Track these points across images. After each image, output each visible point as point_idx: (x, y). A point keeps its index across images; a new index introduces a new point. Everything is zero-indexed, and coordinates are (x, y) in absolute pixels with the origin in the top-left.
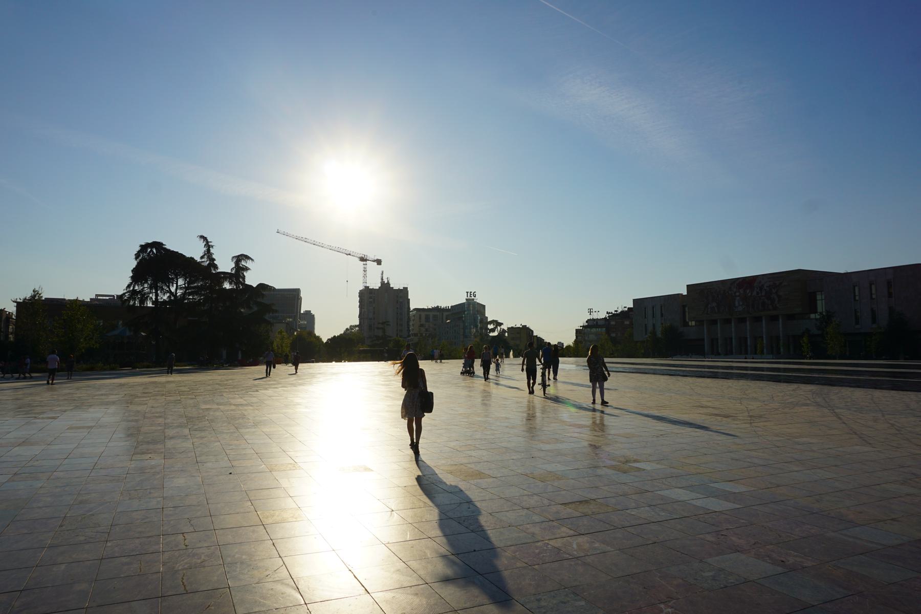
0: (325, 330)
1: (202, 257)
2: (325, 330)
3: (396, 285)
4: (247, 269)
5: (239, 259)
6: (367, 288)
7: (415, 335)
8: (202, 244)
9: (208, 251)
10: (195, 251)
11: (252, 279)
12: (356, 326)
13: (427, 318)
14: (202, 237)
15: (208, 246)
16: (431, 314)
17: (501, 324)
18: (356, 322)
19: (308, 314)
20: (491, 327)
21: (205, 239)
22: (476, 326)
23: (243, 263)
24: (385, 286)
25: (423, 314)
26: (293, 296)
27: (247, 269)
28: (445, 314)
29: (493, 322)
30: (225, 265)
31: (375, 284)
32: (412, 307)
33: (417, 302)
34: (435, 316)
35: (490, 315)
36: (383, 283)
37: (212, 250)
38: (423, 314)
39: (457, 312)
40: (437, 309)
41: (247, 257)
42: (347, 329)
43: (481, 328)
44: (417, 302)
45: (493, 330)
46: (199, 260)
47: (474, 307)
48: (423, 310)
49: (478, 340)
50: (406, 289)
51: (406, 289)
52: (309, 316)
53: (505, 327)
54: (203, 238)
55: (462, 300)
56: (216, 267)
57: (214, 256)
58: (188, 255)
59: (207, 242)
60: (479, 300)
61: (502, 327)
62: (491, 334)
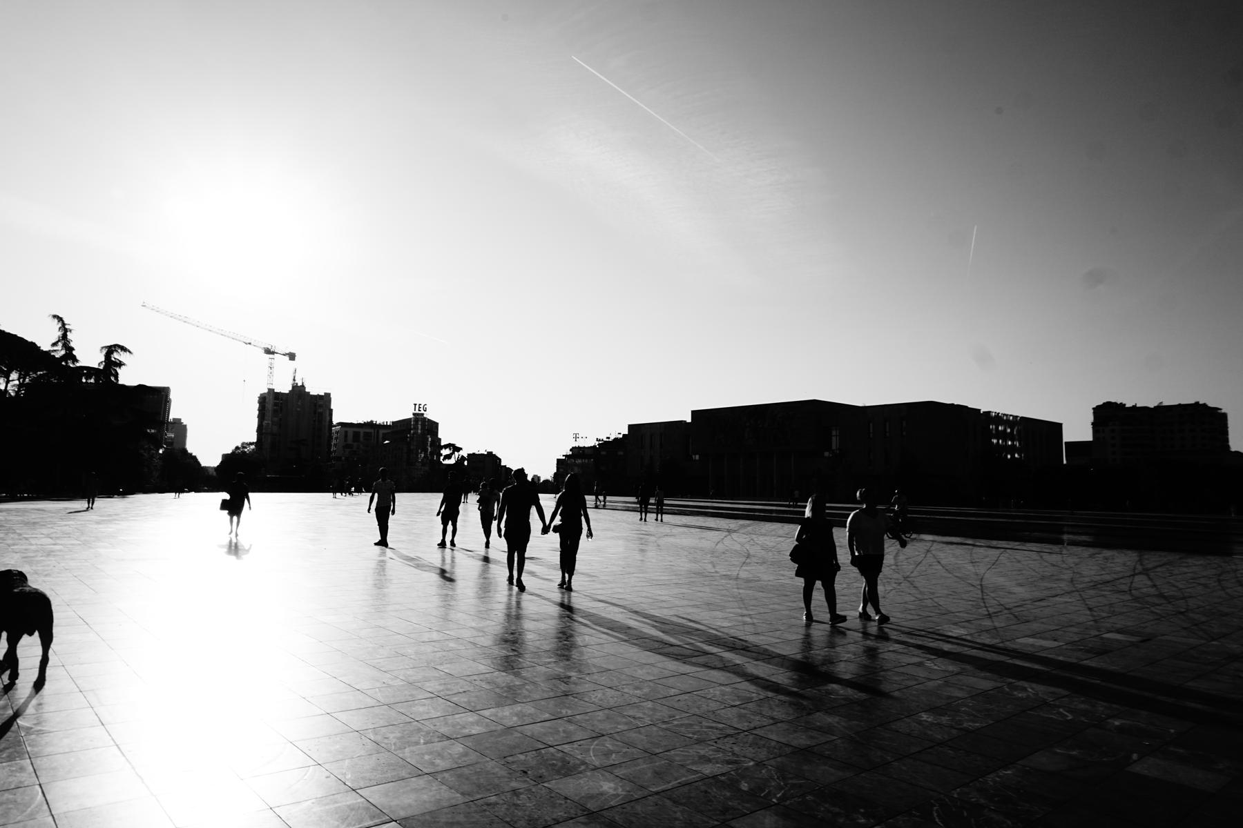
0: (208, 447)
1: (54, 344)
2: (208, 447)
3: (314, 389)
4: (120, 364)
5: (111, 350)
6: (271, 391)
7: (338, 459)
8: (56, 325)
9: (64, 336)
10: (44, 338)
11: (128, 377)
12: (251, 444)
13: (356, 435)
14: (55, 316)
15: (65, 330)
16: (362, 431)
17: (459, 449)
18: (253, 438)
19: (177, 422)
20: (445, 452)
21: (60, 319)
22: (425, 450)
23: (115, 356)
24: (298, 390)
25: (350, 431)
26: (156, 398)
27: (120, 364)
28: (381, 432)
29: (446, 446)
30: (89, 356)
31: (285, 388)
32: (335, 420)
33: (341, 414)
34: (366, 434)
35: (445, 436)
36: (295, 387)
37: (70, 336)
38: (350, 431)
39: (400, 429)
40: (370, 425)
41: (124, 349)
42: (237, 448)
43: (432, 454)
44: (341, 414)
45: (448, 457)
46: (45, 346)
47: (423, 425)
48: (351, 425)
49: (427, 468)
50: (328, 396)
51: (328, 396)
52: (180, 428)
53: (464, 453)
54: (55, 316)
55: (408, 414)
56: (75, 360)
57: (72, 344)
58: (29, 340)
59: (64, 325)
60: (429, 415)
61: (461, 453)
62: (447, 462)
